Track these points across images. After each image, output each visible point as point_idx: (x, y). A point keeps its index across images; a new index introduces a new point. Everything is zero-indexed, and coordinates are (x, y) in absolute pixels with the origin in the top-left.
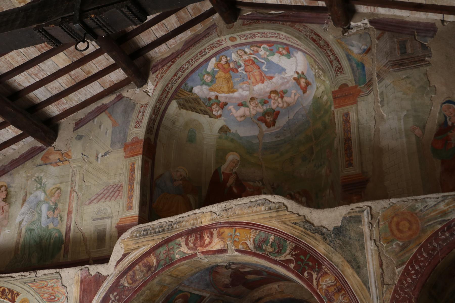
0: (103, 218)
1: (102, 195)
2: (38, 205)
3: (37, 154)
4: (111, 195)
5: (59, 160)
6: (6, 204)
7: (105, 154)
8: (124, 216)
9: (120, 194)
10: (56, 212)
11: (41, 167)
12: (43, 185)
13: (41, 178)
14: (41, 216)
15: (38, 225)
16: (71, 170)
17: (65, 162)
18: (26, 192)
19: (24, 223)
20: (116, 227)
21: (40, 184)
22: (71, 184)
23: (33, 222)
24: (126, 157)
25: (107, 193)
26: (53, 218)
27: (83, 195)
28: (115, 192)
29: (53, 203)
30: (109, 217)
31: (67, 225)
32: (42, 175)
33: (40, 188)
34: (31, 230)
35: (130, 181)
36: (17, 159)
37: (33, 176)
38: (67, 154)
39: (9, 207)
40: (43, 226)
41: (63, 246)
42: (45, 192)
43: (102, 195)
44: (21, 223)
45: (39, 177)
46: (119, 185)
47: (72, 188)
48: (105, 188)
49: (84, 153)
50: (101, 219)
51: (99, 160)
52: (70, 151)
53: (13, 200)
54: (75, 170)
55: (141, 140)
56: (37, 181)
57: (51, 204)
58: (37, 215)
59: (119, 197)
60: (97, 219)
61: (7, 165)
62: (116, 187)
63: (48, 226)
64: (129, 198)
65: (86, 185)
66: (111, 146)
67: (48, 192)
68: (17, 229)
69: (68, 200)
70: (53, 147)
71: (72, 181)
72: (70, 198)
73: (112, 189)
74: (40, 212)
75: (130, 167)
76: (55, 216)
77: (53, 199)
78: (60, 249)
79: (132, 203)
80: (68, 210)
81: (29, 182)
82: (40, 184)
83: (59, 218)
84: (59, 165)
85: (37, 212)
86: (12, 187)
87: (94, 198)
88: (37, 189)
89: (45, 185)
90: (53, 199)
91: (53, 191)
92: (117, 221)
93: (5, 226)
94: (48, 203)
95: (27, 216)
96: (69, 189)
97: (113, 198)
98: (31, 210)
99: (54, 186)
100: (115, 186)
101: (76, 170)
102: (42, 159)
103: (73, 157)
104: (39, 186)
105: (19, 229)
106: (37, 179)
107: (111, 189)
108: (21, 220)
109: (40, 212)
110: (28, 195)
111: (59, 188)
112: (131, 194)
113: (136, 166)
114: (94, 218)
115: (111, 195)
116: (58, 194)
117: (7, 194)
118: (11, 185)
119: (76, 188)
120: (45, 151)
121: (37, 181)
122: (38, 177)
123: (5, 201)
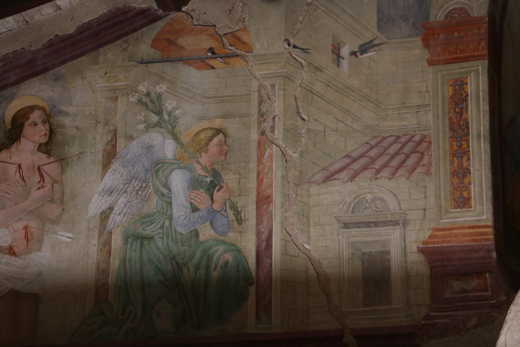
0: (376, 224)
1: (362, 161)
2: (157, 172)
3: (135, 30)
4: (395, 163)
5: (213, 53)
6: (52, 159)
7: (364, 49)
8: (446, 221)
9: (425, 161)
10: (218, 195)
11: (156, 68)
12: (166, 117)
13: (159, 96)
14: (170, 203)
15: (162, 227)
16: (255, 84)
17: (232, 61)
18: (115, 133)
19: (115, 218)
20: (421, 250)
21: (159, 113)
22: (260, 123)
23: (147, 216)
24: (431, 63)
25: (379, 156)
26: (212, 212)
27: (301, 155)
28: (408, 157)
29: (204, 168)
30: (395, 223)
31: (259, 234)
32: (161, 88)
33: (158, 125)
34: (142, 239)
35: (452, 129)
36: (69, 37)
37: (131, 89)
38: (238, 38)
39: (63, 170)
40: (179, 229)
41: (252, 290)
42: (176, 138)
43: (362, 161)
44: (105, 216)
45: (153, 95)
46: (417, 138)
47: (263, 133)
48: (373, 143)
49: (292, 41)
50: (368, 224)
51: (345, 64)
52: (245, 29)
53: (73, 150)
54: (267, 83)
55: (481, 18)
56: (146, 105)
57: (200, 171)
58: (155, 198)
59: (419, 169)
60: (358, 225)
61: (38, 51)
62: (409, 141)
63: (196, 234)
64: (454, 174)
65: (309, 130)
66: (379, 28)
67: (185, 139)
68: (97, 232)
69: (253, 165)
70: (187, 13)
71: (261, 115)
72: (260, 161)
73: (396, 147)
74: (165, 191)
75: (449, 91)
76: (216, 206)
77: (204, 159)
78: (242, 297)
79: (467, 188)
80: (258, 193)
81: (121, 105)
82: (159, 113)
83: (230, 213)
84: (213, 68)
85: (157, 191)
86: (66, 114)
87: (338, 166)
88: (149, 126)
89: (174, 121)
90: (204, 159)
91: (202, 136)
92: (424, 235)
93: (56, 221)
94: (190, 171)
95: (122, 200)
96: (255, 136)
97: (401, 172)
98: (136, 184)
99: (205, 124)
100: (403, 140)
101: (273, 86)
102: (155, 44)
103: (258, 48)
104: (155, 118)
105: (101, 234)
106: (145, 99)
107: (391, 145)
108: (105, 207)
109: (165, 191)
110: (121, 143)
111: (218, 131)
112: (460, 166)
113: (470, 88)
114: (346, 220)
115: (395, 163)
116: (220, 145)
117: (52, 133)
118: (63, 108)
119: (279, 135)
120: (160, 25)
121: (146, 105)
122: (148, 94)
123: (48, 153)
